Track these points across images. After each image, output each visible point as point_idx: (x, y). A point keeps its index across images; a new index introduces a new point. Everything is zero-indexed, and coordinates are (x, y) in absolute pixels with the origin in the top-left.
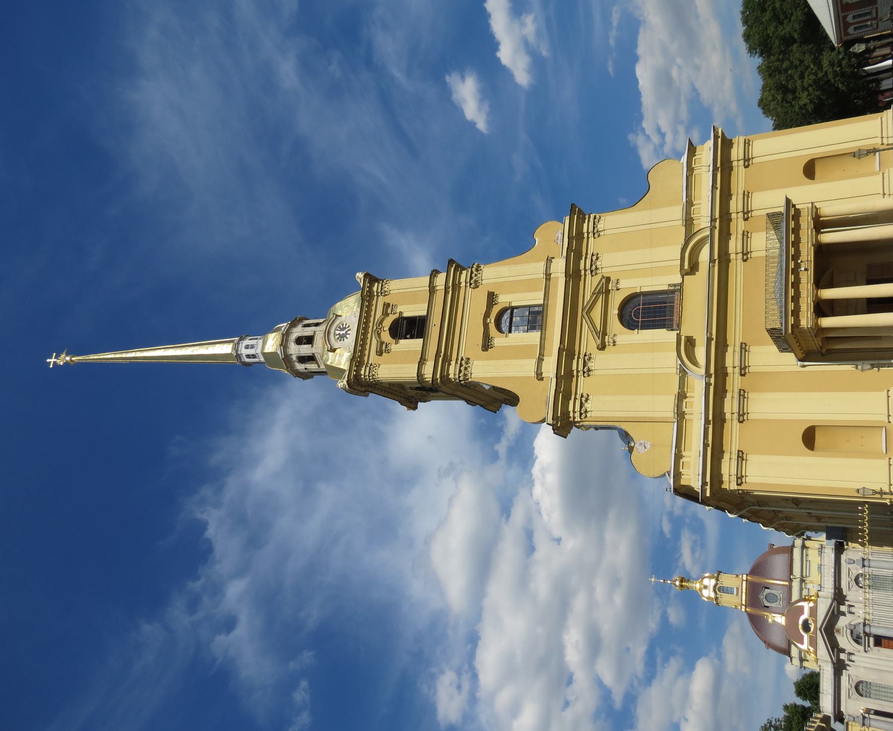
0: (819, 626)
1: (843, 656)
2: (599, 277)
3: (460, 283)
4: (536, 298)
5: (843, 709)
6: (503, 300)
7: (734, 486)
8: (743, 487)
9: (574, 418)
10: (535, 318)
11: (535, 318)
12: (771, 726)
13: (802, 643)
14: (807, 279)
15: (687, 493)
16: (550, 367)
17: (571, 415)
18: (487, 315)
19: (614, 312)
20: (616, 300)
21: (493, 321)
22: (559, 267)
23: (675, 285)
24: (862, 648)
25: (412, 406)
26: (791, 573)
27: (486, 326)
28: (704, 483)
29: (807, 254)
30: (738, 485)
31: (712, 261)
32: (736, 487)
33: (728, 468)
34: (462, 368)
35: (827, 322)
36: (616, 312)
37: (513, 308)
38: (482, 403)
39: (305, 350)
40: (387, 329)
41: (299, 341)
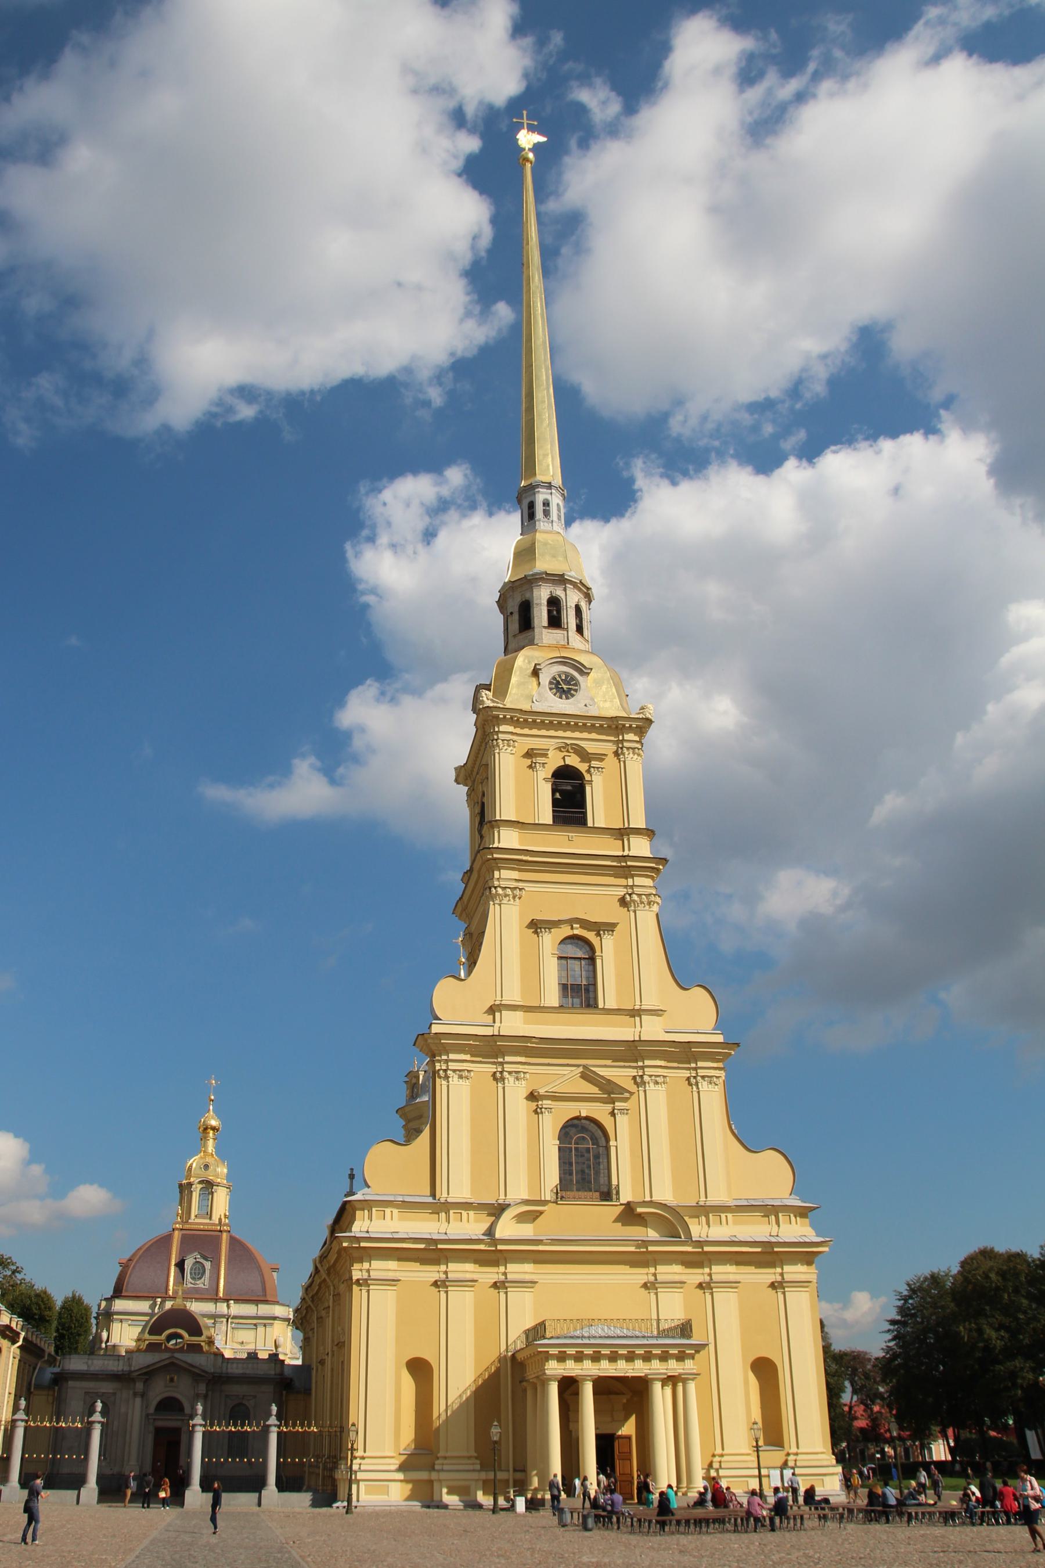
0: (177, 1355)
1: (140, 1386)
2: (632, 1088)
3: (632, 876)
4: (609, 995)
5: (71, 1383)
6: (607, 948)
7: (356, 1275)
8: (355, 1288)
9: (439, 1061)
10: (581, 994)
11: (581, 994)
12: (14, 1272)
13: (151, 1333)
14: (607, 1369)
15: (344, 1216)
16: (512, 1024)
17: (444, 1057)
18: (585, 924)
19: (585, 1110)
20: (599, 1111)
21: (576, 932)
22: (652, 1029)
23: (618, 1193)
24: (152, 1410)
25: (462, 775)
26: (237, 1301)
27: (571, 922)
28: (358, 1239)
29: (638, 1369)
30: (358, 1280)
31: (645, 1243)
32: (355, 1278)
33: (380, 1268)
34: (509, 892)
35: (554, 1389)
36: (584, 1114)
37: (592, 960)
38: (466, 898)
39: (541, 615)
40: (569, 761)
41: (554, 603)
